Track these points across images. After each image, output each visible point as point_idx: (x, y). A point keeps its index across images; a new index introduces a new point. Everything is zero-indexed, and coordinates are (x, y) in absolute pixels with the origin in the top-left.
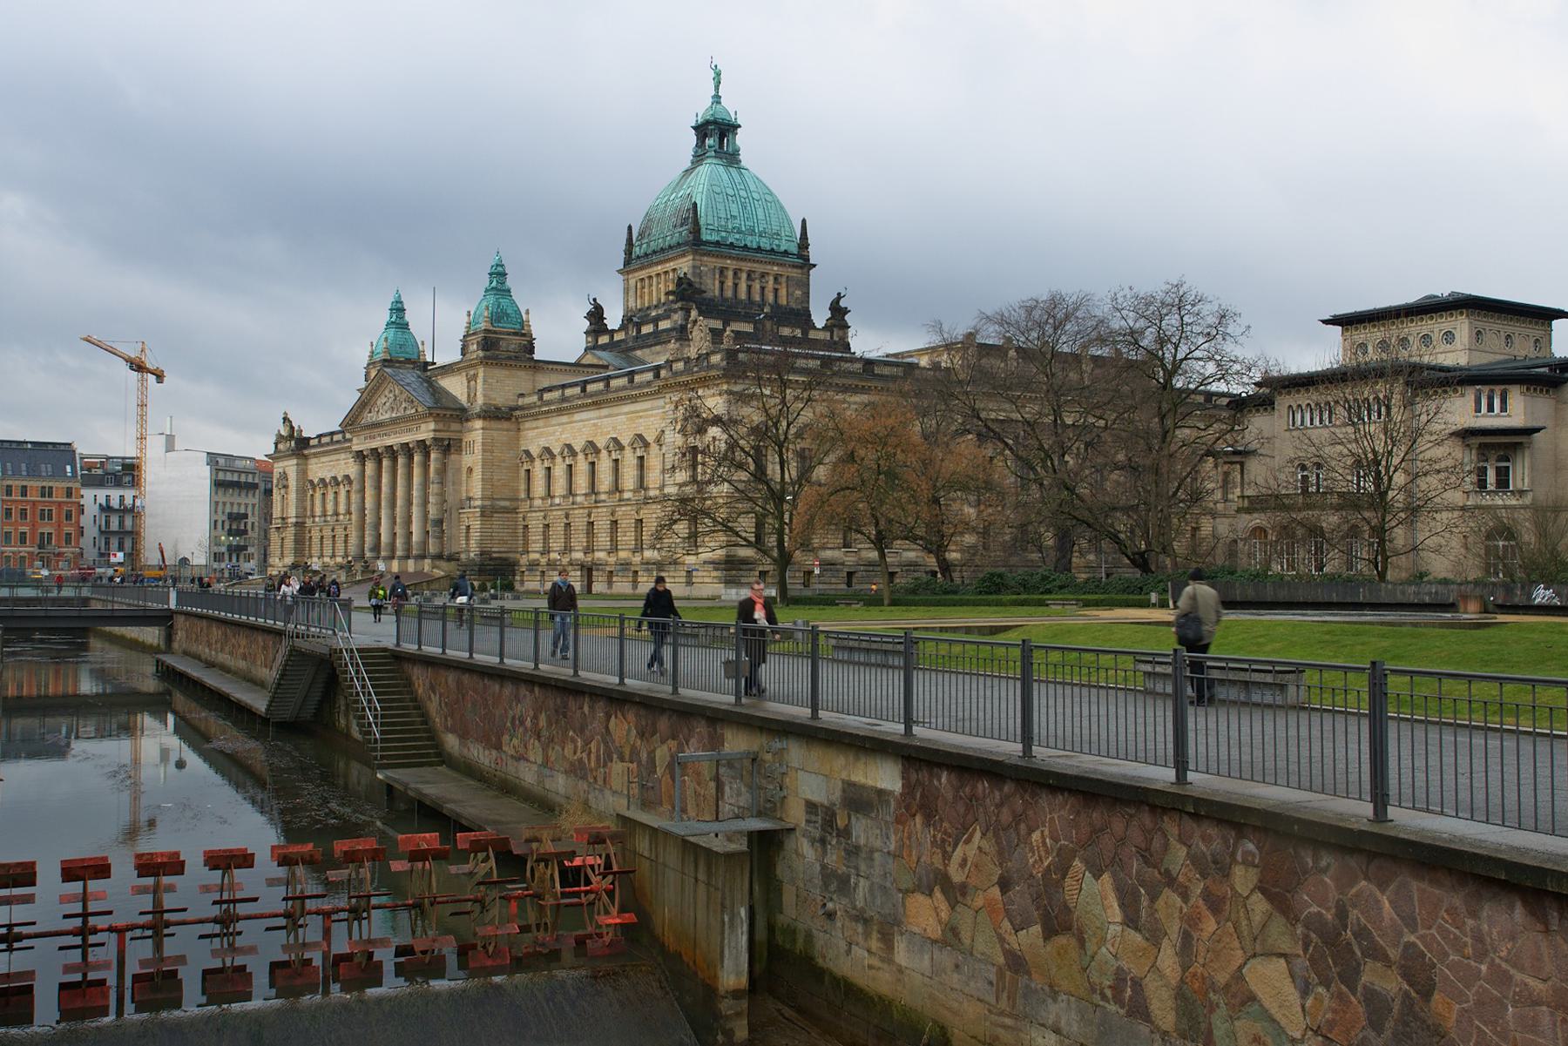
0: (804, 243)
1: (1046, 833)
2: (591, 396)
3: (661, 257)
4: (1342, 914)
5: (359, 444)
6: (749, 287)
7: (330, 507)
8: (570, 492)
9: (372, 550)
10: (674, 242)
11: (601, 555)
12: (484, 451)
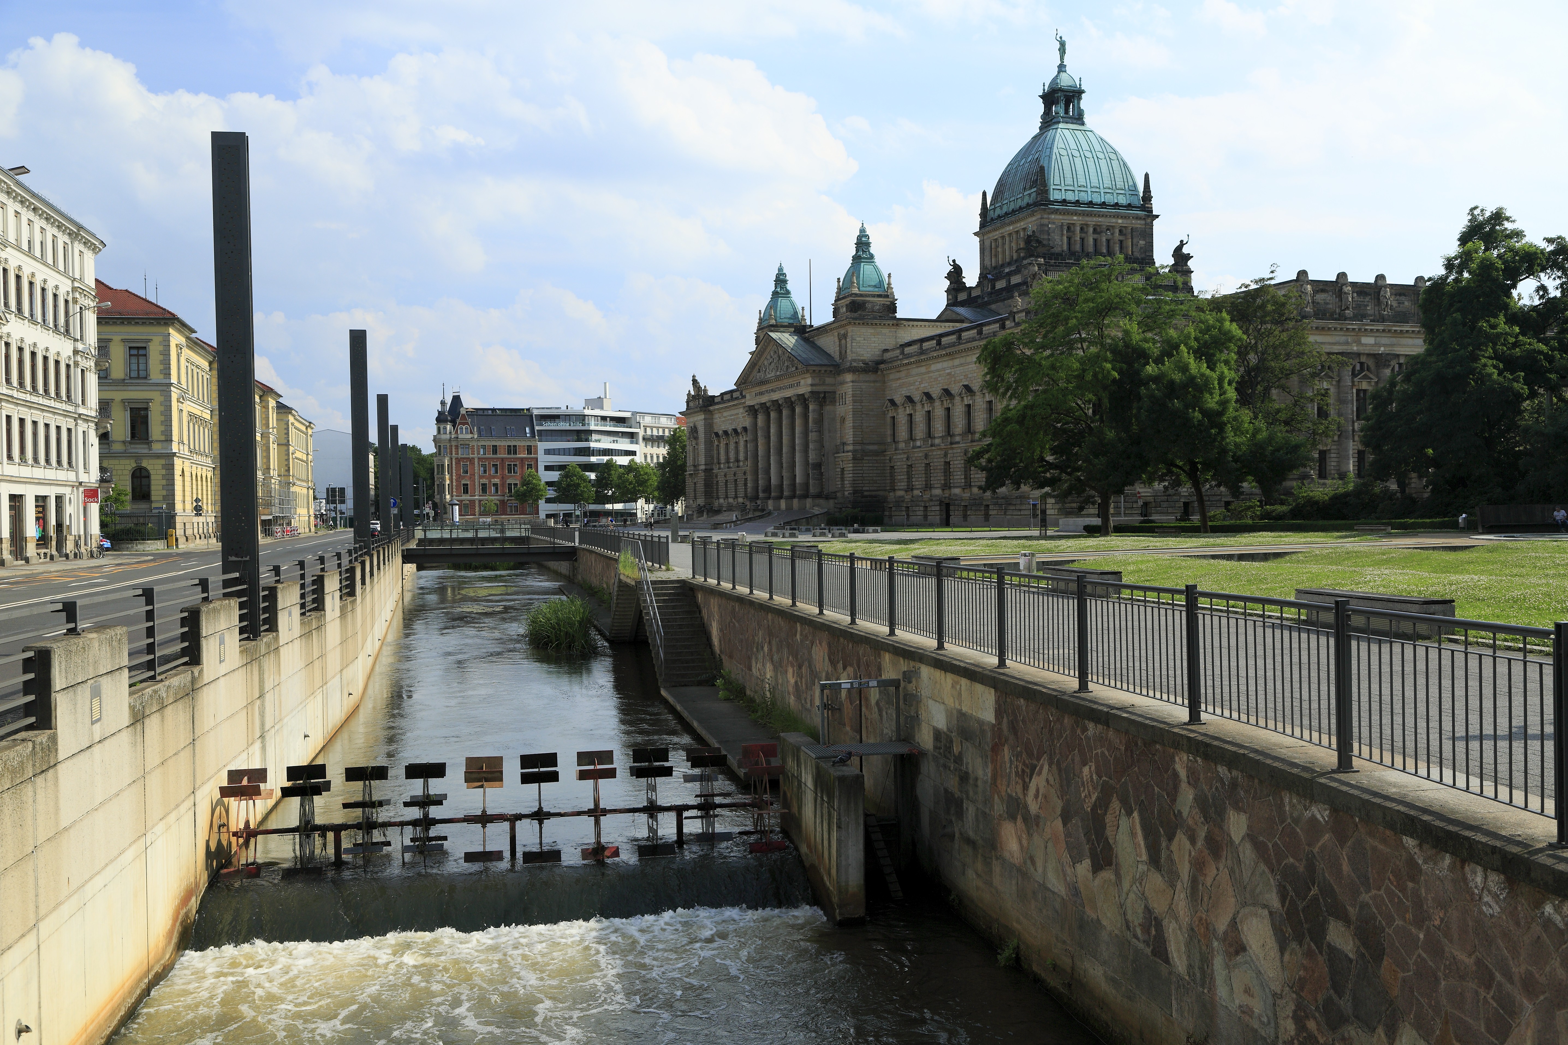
0: (1147, 196)
1: (1093, 768)
3: (1013, 218)
4: (1311, 867)
5: (751, 400)
6: (1095, 240)
7: (732, 455)
8: (929, 435)
9: (764, 491)
10: (1024, 203)
11: (957, 491)
12: (854, 401)
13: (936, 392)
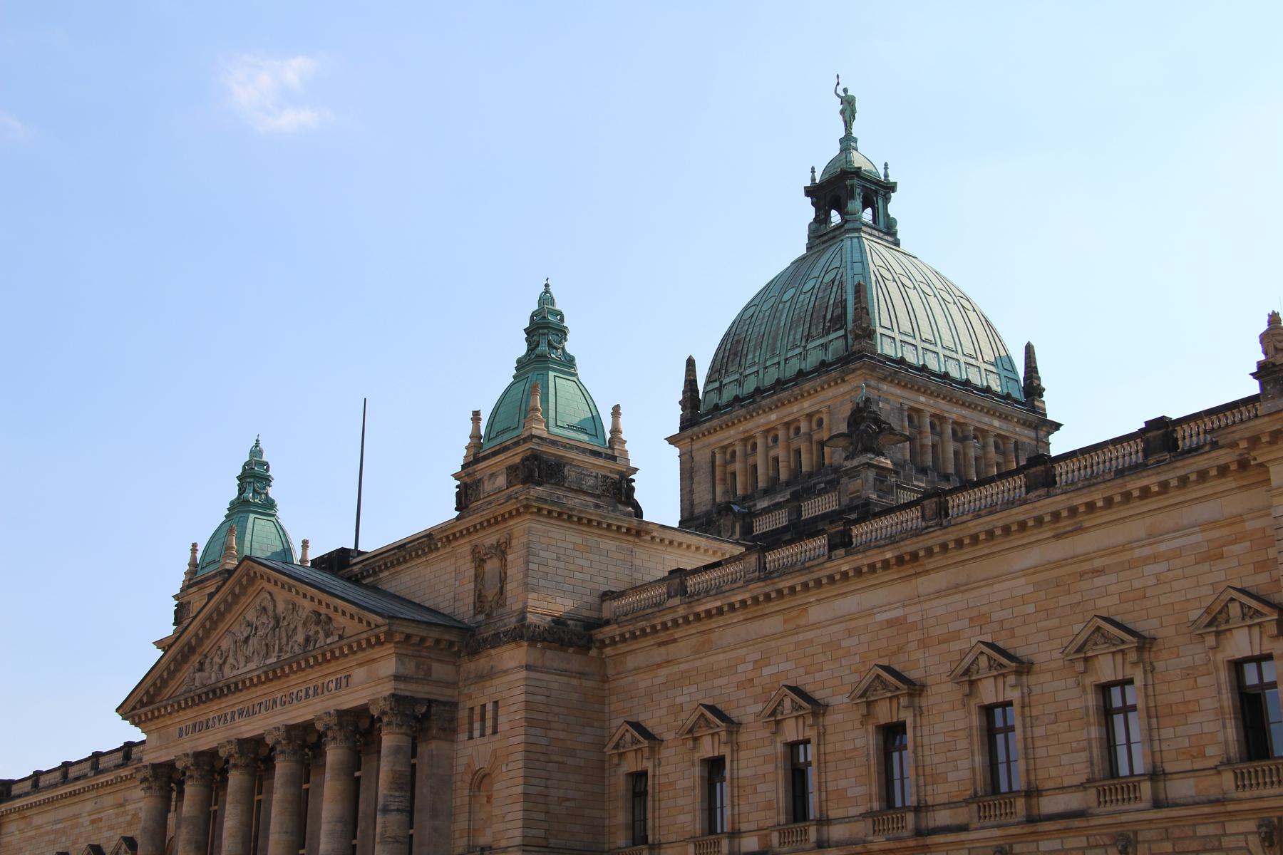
0: (1033, 389)
2: (867, 547)
6: (956, 453)
13: (836, 682)
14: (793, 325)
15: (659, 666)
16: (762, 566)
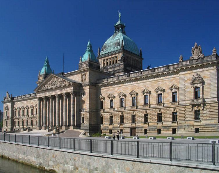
13: (127, 92)
14: (113, 44)
15: (105, 89)
16: (118, 78)
